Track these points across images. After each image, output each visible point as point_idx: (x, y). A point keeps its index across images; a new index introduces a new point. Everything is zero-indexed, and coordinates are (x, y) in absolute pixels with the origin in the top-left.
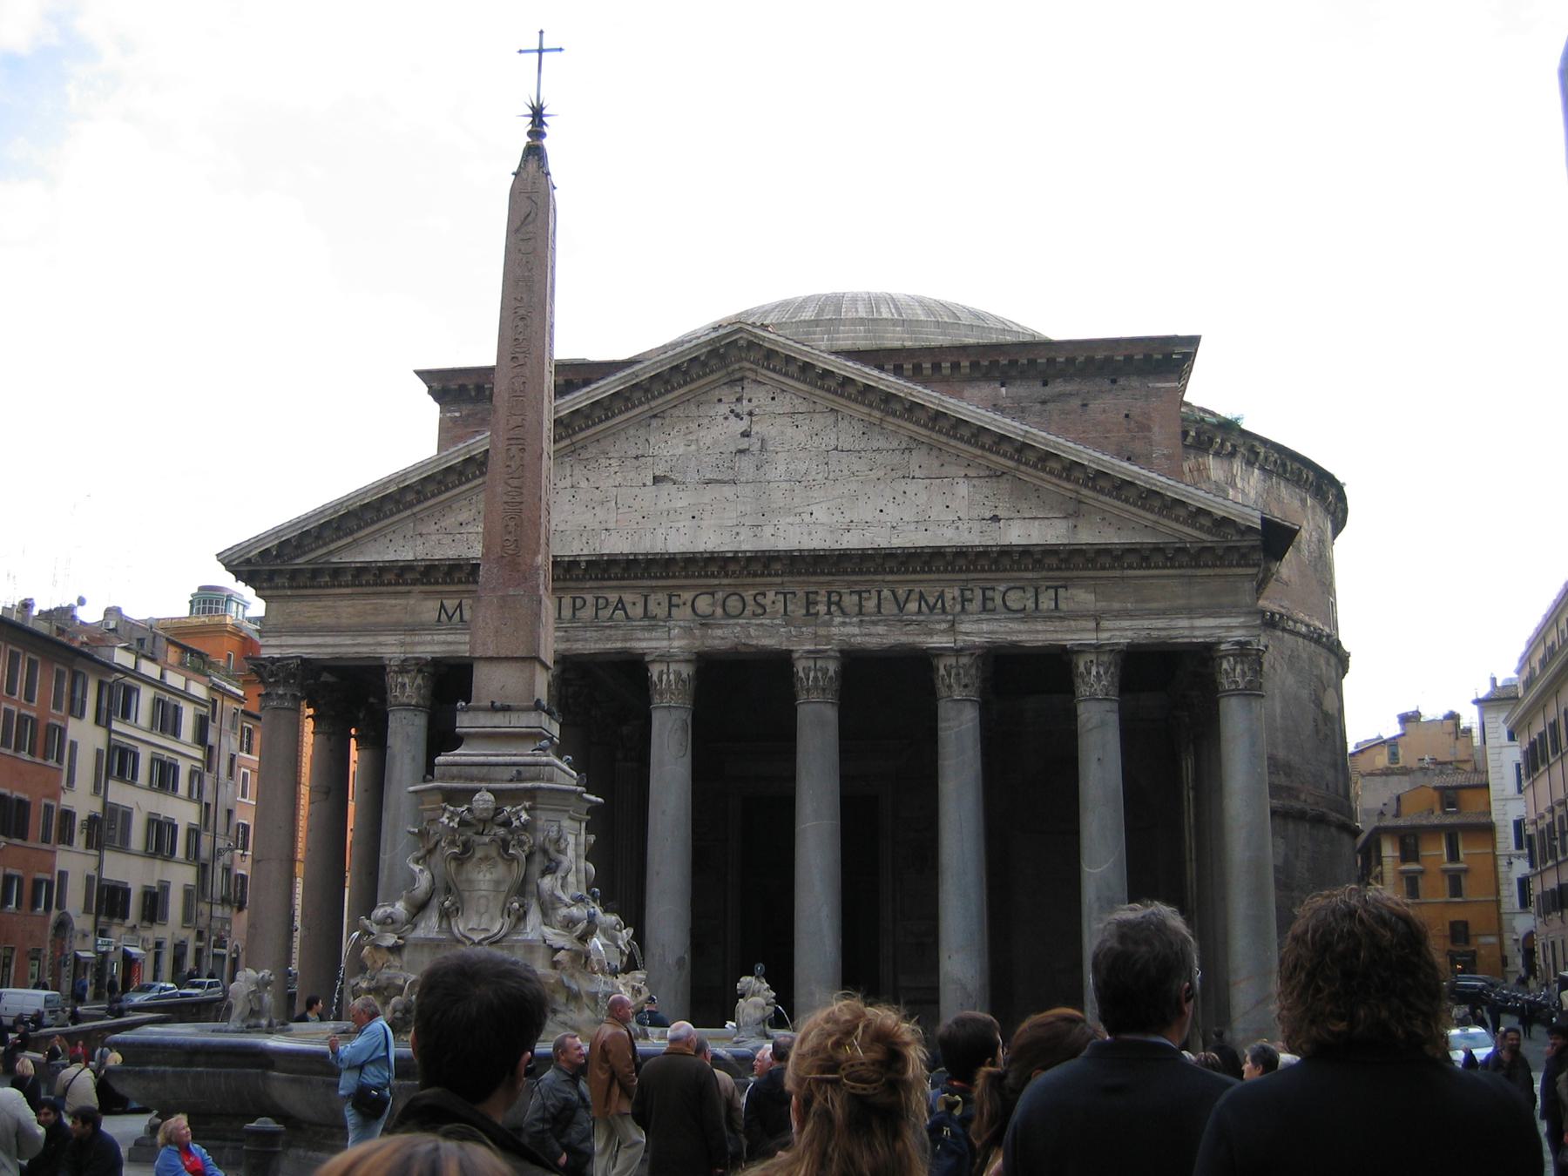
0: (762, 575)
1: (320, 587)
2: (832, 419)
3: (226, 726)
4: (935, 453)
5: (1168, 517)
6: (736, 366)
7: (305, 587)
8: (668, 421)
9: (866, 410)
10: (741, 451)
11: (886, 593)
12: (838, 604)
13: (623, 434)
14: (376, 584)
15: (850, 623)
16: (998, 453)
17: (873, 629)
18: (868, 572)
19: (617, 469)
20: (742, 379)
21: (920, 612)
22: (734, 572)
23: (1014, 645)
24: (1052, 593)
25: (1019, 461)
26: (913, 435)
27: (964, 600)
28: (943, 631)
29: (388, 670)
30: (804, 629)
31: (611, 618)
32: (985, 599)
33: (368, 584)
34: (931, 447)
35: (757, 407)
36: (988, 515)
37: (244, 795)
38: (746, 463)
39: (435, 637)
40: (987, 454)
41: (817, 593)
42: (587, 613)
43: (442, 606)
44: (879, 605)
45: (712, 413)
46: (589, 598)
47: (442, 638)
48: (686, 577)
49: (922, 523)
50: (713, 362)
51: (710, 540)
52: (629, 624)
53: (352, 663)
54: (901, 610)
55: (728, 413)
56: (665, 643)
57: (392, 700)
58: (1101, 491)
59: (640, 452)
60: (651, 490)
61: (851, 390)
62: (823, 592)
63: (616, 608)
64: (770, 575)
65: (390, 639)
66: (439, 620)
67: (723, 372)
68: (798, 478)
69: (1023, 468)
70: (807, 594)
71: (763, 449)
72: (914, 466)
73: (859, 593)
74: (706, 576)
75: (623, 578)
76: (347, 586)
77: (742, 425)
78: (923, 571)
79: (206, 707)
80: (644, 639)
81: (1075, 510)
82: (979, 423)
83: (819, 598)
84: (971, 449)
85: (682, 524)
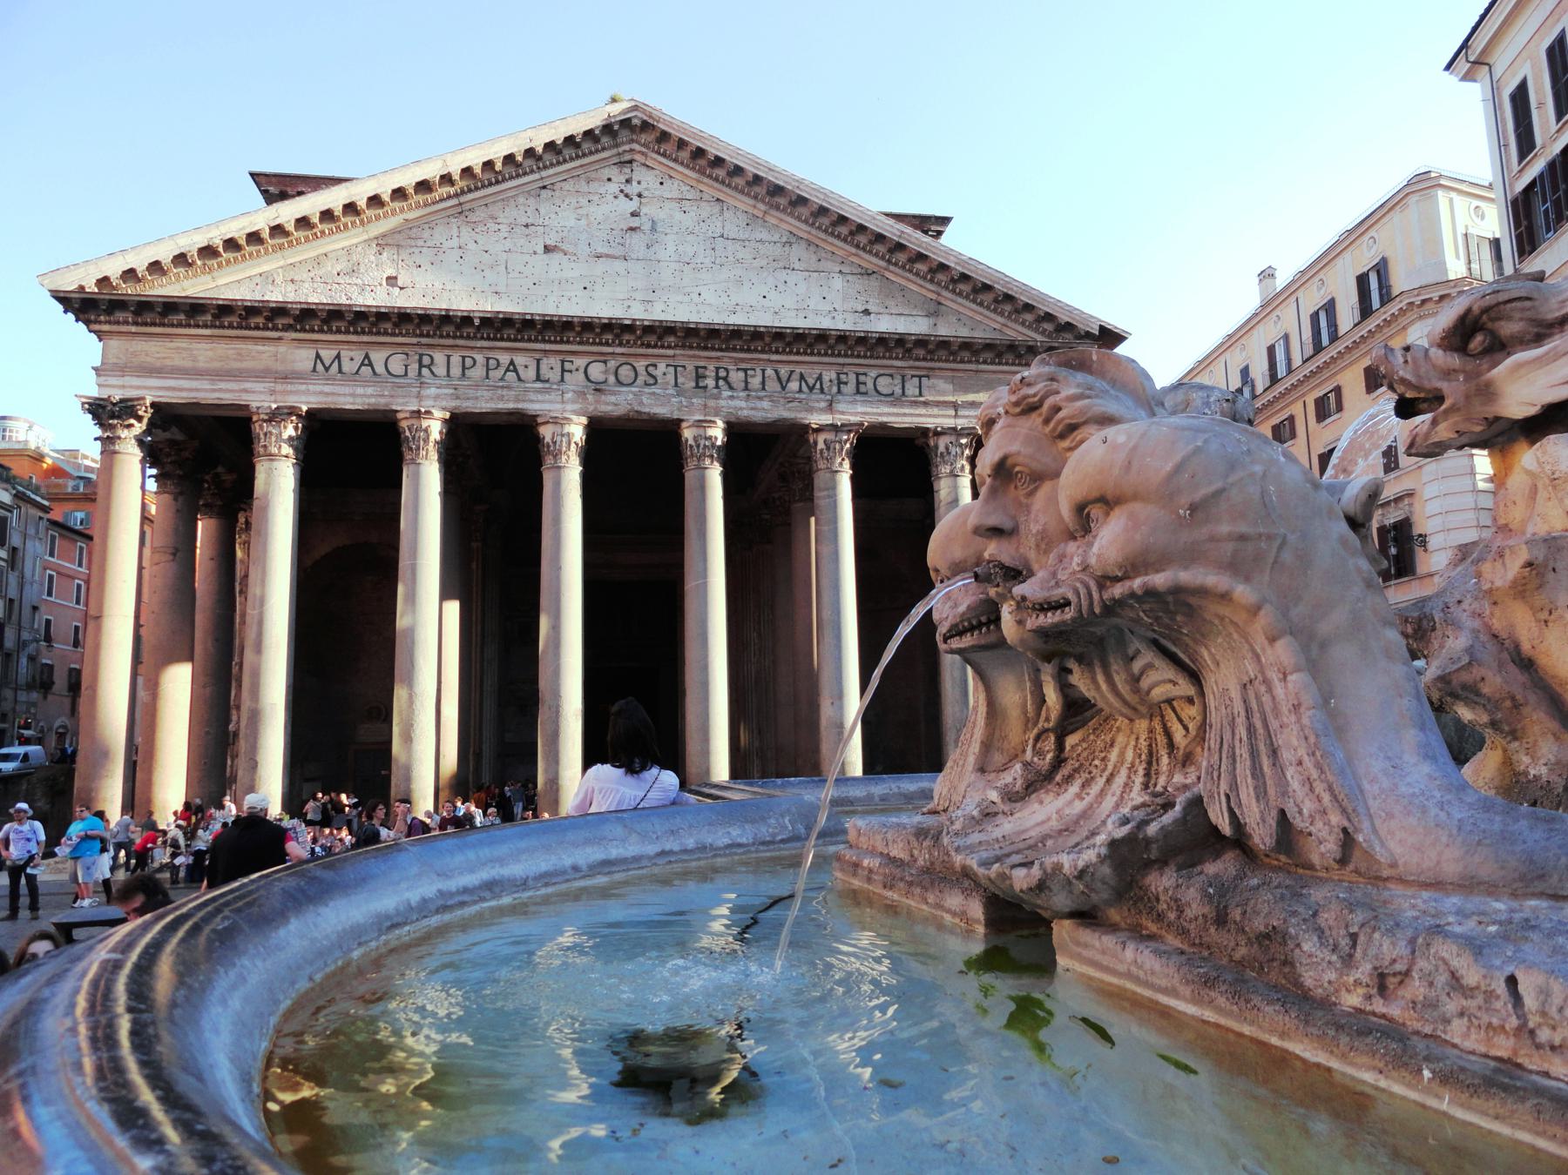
0: (655, 346)
1: (172, 325)
2: (717, 208)
3: (31, 531)
4: (812, 248)
5: (1016, 321)
6: (627, 147)
7: (154, 324)
8: (557, 193)
9: (752, 202)
10: (632, 229)
11: (770, 372)
12: (725, 379)
13: (512, 203)
14: (240, 327)
15: (738, 397)
16: (870, 252)
17: (759, 404)
18: (756, 351)
19: (506, 235)
20: (630, 162)
21: (800, 391)
22: (628, 342)
23: (883, 426)
24: (916, 380)
25: (889, 261)
26: (794, 230)
27: (840, 383)
28: (822, 410)
29: (255, 418)
30: (694, 400)
31: (502, 379)
32: (858, 383)
33: (231, 326)
34: (809, 243)
35: (646, 189)
36: (861, 308)
37: (50, 594)
38: (637, 242)
39: (311, 387)
40: (861, 253)
41: (705, 368)
42: (477, 372)
43: (318, 356)
44: (763, 383)
45: (602, 191)
46: (479, 358)
47: (319, 388)
48: (580, 343)
49: (799, 310)
50: (605, 140)
51: (602, 309)
52: (522, 385)
53: (206, 413)
54: (784, 388)
55: (618, 193)
56: (559, 406)
57: (261, 450)
58: (960, 294)
59: (530, 221)
60: (542, 258)
61: (739, 181)
62: (711, 367)
63: (508, 370)
64: (663, 347)
65: (259, 387)
66: (314, 370)
67: (615, 151)
68: (687, 260)
69: (892, 268)
70: (697, 368)
71: (653, 229)
72: (794, 259)
73: (745, 370)
74: (601, 344)
75: (515, 340)
76: (206, 326)
77: (633, 205)
78: (805, 353)
79: (11, 512)
80: (538, 401)
81: (935, 310)
82: (859, 221)
83: (707, 373)
84: (847, 247)
85: (573, 294)
